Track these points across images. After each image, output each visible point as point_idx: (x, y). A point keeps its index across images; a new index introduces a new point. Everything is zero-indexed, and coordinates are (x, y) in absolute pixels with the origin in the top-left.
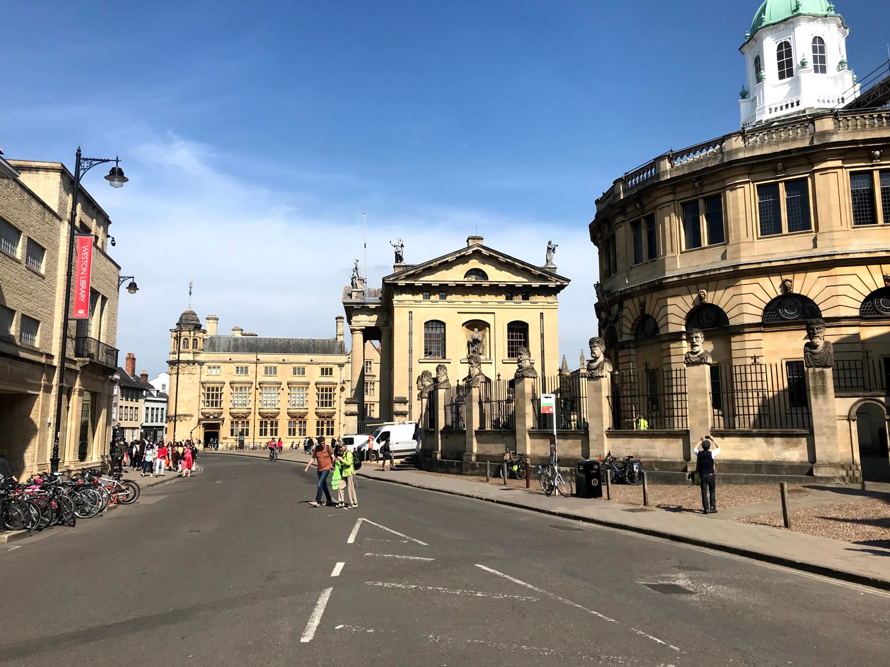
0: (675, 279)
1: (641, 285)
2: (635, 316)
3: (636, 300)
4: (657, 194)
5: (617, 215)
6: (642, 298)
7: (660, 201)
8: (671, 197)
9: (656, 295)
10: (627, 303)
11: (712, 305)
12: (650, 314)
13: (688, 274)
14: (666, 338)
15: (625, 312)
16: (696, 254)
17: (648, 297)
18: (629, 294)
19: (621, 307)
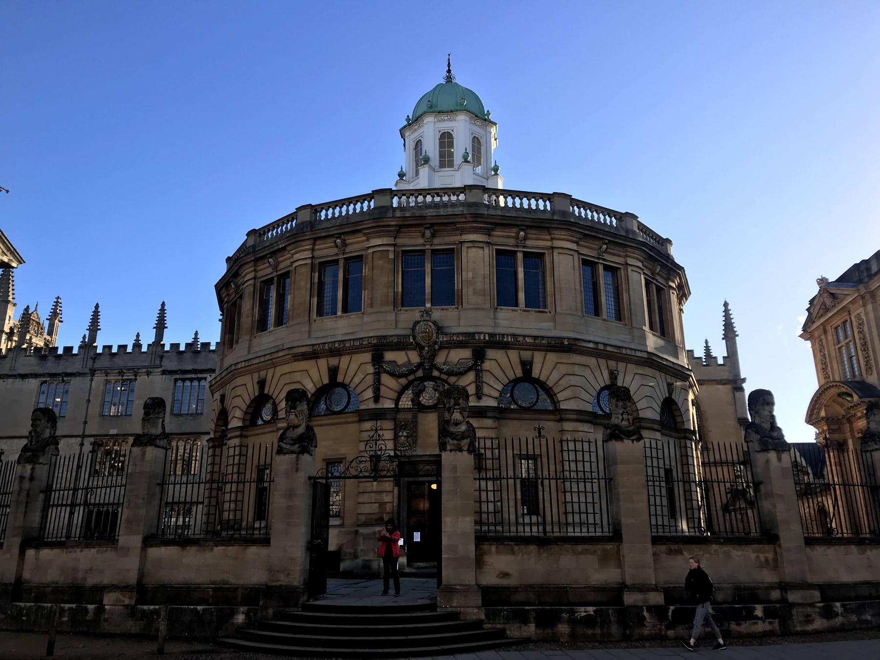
0: (591, 345)
1: (535, 337)
2: (512, 377)
3: (514, 355)
4: (562, 234)
5: (476, 230)
6: (526, 355)
7: (557, 243)
8: (574, 246)
9: (552, 357)
10: (491, 353)
11: (622, 387)
12: (543, 378)
13: (605, 345)
14: (574, 417)
15: (487, 365)
16: (597, 322)
17: (538, 357)
18: (507, 343)
19: (479, 356)
